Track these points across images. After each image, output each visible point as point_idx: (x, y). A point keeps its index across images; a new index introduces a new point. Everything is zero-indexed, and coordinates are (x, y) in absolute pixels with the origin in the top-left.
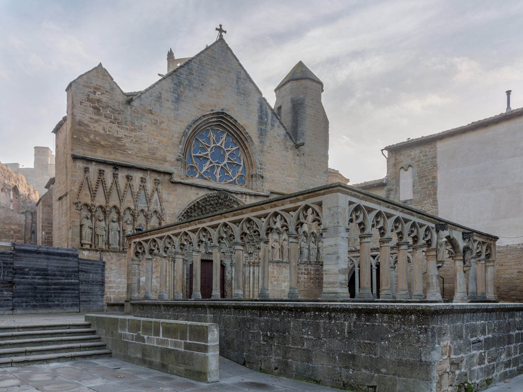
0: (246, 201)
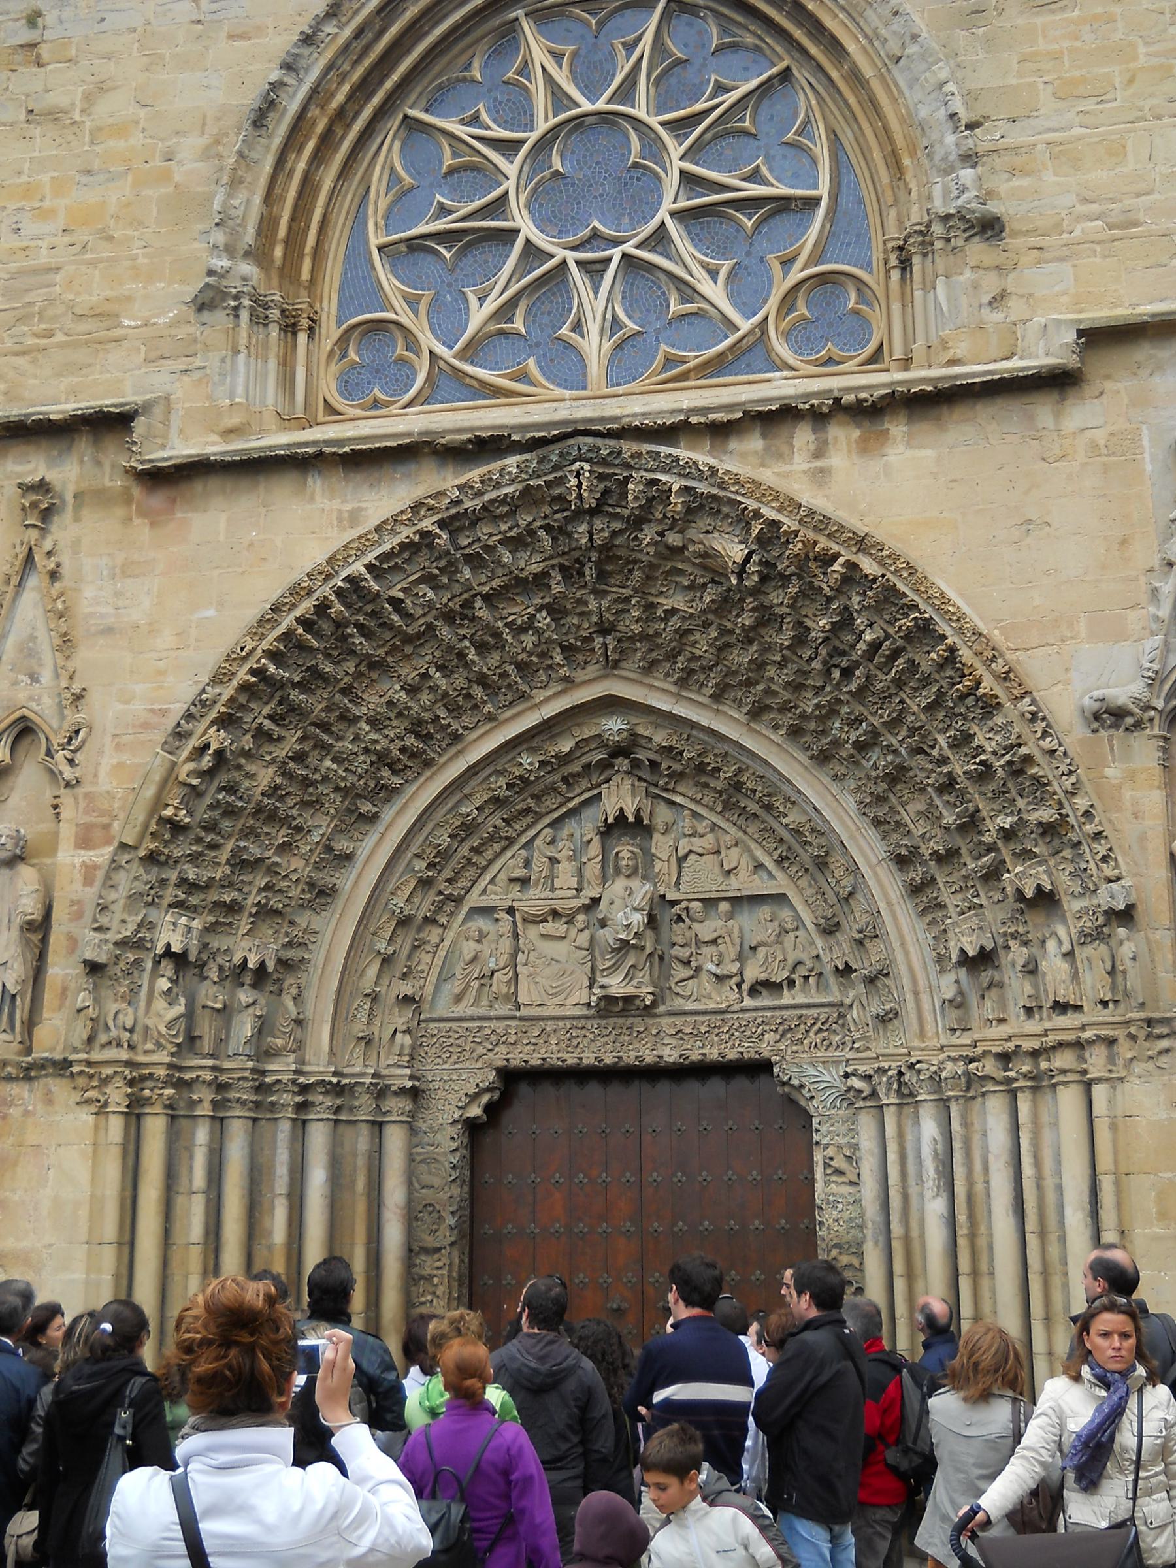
0: (820, 476)
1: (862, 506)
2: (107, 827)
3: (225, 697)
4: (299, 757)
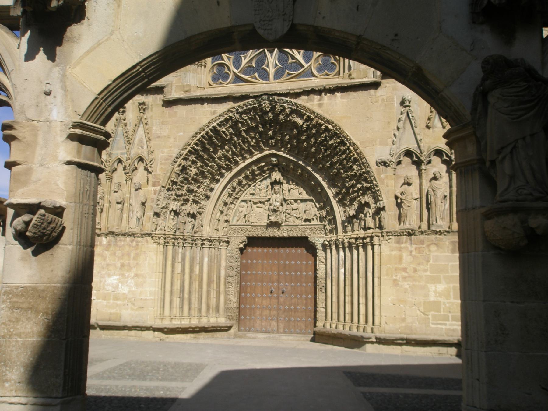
0: (320, 105)
1: (330, 113)
2: (159, 182)
3: (185, 154)
4: (202, 167)
